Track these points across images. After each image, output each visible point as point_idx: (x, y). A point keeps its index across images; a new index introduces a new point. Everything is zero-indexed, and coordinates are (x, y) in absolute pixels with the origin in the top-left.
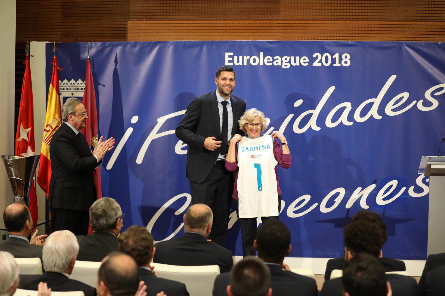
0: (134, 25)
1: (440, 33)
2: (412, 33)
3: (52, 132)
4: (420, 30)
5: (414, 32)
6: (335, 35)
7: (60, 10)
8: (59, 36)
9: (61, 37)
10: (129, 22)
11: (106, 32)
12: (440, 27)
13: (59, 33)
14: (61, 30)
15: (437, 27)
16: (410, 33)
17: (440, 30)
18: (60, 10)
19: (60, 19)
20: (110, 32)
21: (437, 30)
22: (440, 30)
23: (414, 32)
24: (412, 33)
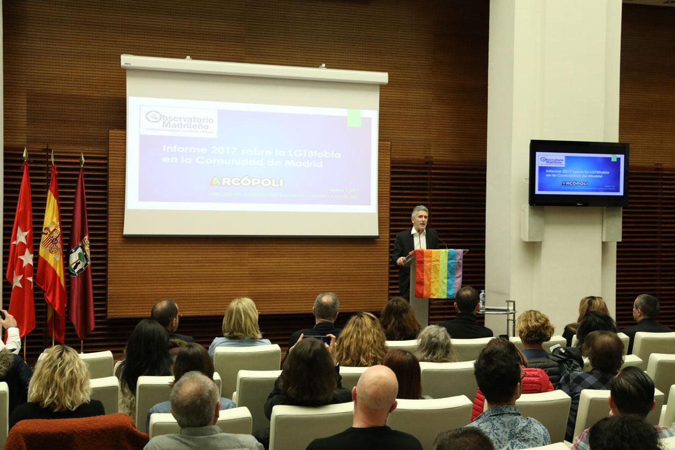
0: (115, 135)
3: (49, 235)
7: (26, 114)
8: (26, 140)
9: (27, 142)
10: (110, 131)
11: (78, 140)
13: (25, 138)
18: (26, 114)
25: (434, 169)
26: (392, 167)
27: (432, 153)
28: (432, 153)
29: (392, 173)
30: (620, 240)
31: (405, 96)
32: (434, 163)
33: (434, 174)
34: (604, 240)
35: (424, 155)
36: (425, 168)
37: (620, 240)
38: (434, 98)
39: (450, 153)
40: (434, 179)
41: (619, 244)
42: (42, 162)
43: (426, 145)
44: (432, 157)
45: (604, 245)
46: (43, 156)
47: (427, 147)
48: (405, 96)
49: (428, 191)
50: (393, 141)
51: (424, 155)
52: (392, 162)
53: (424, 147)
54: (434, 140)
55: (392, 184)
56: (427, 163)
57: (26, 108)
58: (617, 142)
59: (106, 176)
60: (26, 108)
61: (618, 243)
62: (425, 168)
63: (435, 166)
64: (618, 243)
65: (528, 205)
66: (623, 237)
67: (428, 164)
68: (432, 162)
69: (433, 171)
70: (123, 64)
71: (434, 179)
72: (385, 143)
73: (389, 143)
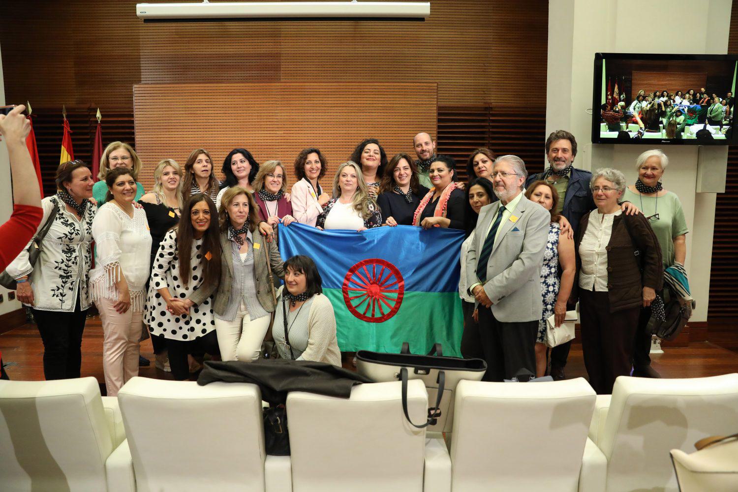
1: (427, 94)
2: (402, 93)
4: (408, 90)
5: (403, 93)
6: (330, 96)
12: (428, 88)
13: (75, 100)
14: (76, 97)
15: (425, 88)
16: (400, 93)
17: (428, 91)
19: (75, 86)
20: (124, 99)
21: (425, 91)
22: (428, 91)
23: (403, 93)
24: (402, 93)
25: (493, 115)
26: (439, 114)
27: (492, 98)
28: (492, 98)
29: (439, 121)
30: (723, 191)
31: (461, 36)
32: (494, 109)
33: (493, 121)
34: (699, 191)
35: (483, 101)
36: (485, 115)
37: (722, 190)
38: (494, 37)
39: (513, 99)
40: (493, 127)
41: (720, 196)
42: (86, 122)
43: (485, 90)
44: (491, 103)
45: (699, 198)
46: (87, 116)
47: (486, 92)
48: (461, 36)
49: (486, 140)
50: (439, 84)
51: (483, 101)
52: (439, 108)
53: (482, 93)
54: (494, 84)
55: (439, 133)
56: (486, 109)
57: (74, 72)
58: (725, 52)
59: (133, 134)
60: (74, 72)
61: (718, 194)
62: (485, 115)
63: (493, 112)
64: (718, 194)
65: (591, 143)
66: (726, 188)
67: (487, 110)
68: (491, 108)
69: (491, 118)
70: (138, 13)
71: (493, 127)
72: (430, 84)
73: (436, 85)
